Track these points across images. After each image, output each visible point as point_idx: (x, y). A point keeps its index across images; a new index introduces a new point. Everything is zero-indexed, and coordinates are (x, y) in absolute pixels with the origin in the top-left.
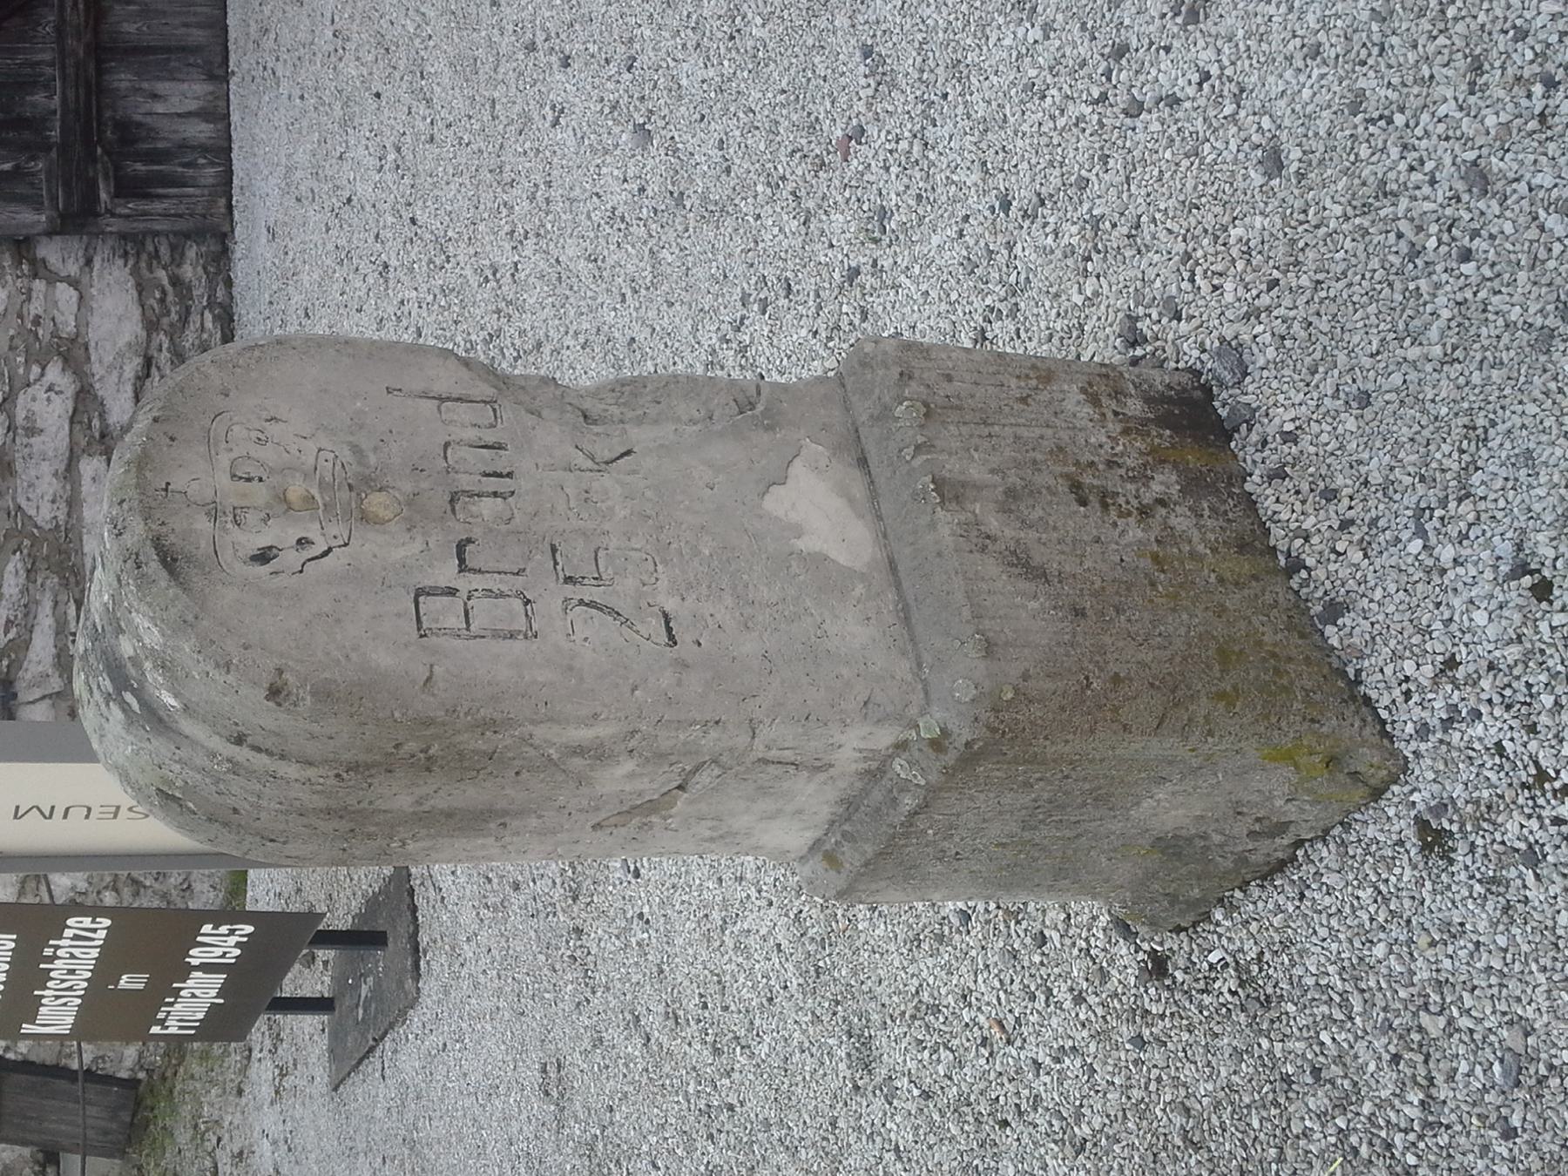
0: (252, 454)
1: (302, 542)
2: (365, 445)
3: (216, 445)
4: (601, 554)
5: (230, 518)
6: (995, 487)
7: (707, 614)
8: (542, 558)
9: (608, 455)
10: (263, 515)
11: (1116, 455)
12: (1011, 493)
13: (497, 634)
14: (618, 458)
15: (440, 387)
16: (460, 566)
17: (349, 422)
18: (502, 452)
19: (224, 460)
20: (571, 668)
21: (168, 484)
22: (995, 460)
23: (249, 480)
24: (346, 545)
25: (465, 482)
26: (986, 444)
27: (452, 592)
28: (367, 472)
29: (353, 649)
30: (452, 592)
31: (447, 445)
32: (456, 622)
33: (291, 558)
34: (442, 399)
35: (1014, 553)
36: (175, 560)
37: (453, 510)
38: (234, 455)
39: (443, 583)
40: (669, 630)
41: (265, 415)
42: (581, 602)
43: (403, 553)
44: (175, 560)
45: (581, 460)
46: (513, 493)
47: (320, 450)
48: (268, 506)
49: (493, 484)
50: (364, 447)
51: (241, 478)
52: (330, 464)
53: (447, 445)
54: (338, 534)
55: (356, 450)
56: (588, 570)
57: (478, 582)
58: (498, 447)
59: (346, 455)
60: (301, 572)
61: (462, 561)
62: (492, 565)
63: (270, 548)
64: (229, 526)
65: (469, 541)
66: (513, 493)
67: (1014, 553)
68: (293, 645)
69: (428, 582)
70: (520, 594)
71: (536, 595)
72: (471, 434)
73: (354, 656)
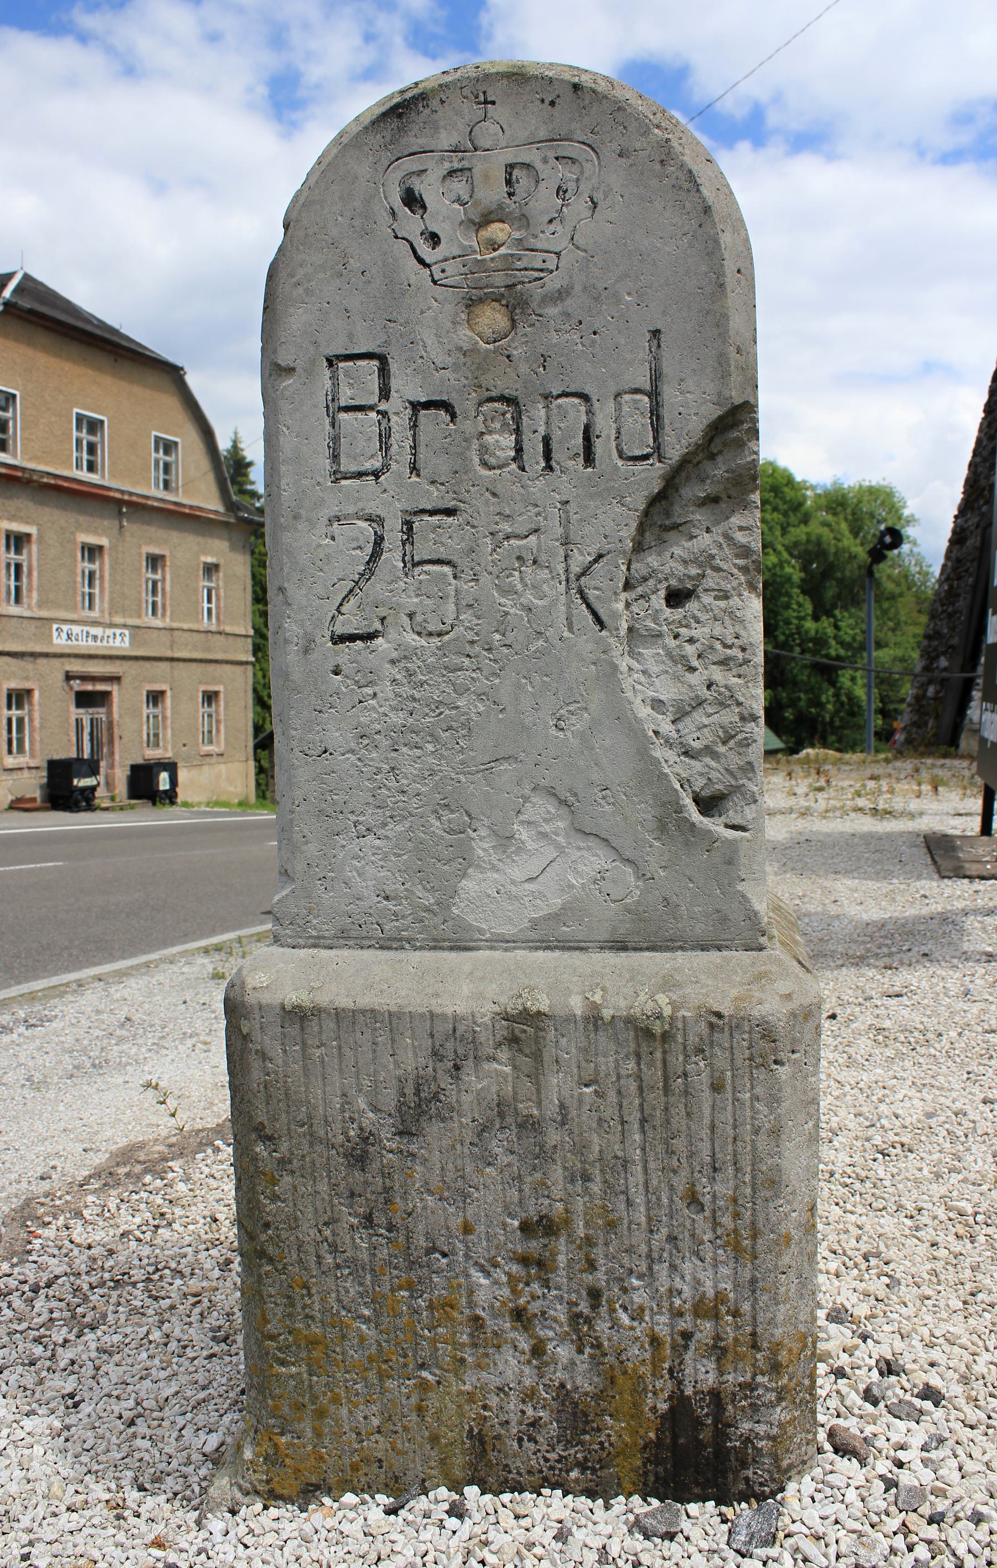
0: (543, 185)
1: (434, 239)
2: (570, 304)
3: (552, 147)
4: (446, 569)
5: (456, 165)
6: (539, 1104)
7: (377, 689)
8: (435, 497)
9: (592, 594)
10: (466, 197)
11: (612, 1310)
12: (529, 1125)
13: (336, 439)
14: (589, 606)
15: (669, 394)
16: (419, 403)
17: (601, 286)
18: (581, 460)
19: (531, 155)
20: (296, 517)
21: (493, 103)
22: (584, 1118)
23: (509, 182)
24: (434, 282)
25: (536, 416)
26: (609, 1112)
27: (385, 393)
28: (534, 305)
29: (307, 291)
30: (385, 393)
31: (585, 397)
32: (346, 396)
33: (412, 224)
34: (654, 394)
35: (436, 1097)
36: (400, 116)
37: (491, 400)
38: (538, 165)
39: (394, 384)
40: (352, 638)
41: (598, 197)
42: (379, 540)
43: (429, 342)
44: (400, 116)
45: (579, 560)
46: (523, 469)
47: (558, 254)
48: (476, 204)
49: (534, 448)
50: (569, 302)
51: (510, 174)
52: (539, 265)
53: (585, 397)
54: (448, 274)
55: (561, 295)
56: (423, 550)
57: (400, 423)
58: (589, 458)
59: (553, 283)
60: (396, 237)
61: (428, 405)
62: (422, 438)
63: (424, 207)
64: (447, 165)
65: (453, 416)
66: (523, 469)
67: (436, 1097)
68: (311, 232)
69: (394, 367)
70: (386, 467)
71: (385, 485)
72: (604, 425)
73: (300, 290)
